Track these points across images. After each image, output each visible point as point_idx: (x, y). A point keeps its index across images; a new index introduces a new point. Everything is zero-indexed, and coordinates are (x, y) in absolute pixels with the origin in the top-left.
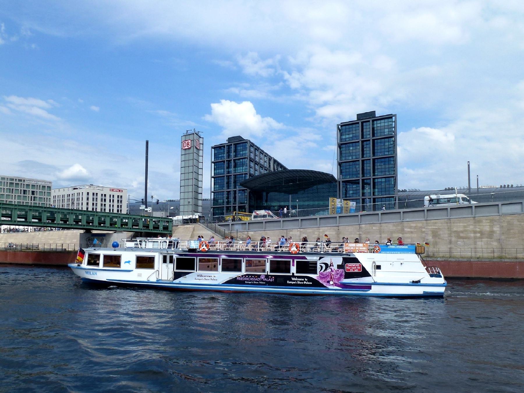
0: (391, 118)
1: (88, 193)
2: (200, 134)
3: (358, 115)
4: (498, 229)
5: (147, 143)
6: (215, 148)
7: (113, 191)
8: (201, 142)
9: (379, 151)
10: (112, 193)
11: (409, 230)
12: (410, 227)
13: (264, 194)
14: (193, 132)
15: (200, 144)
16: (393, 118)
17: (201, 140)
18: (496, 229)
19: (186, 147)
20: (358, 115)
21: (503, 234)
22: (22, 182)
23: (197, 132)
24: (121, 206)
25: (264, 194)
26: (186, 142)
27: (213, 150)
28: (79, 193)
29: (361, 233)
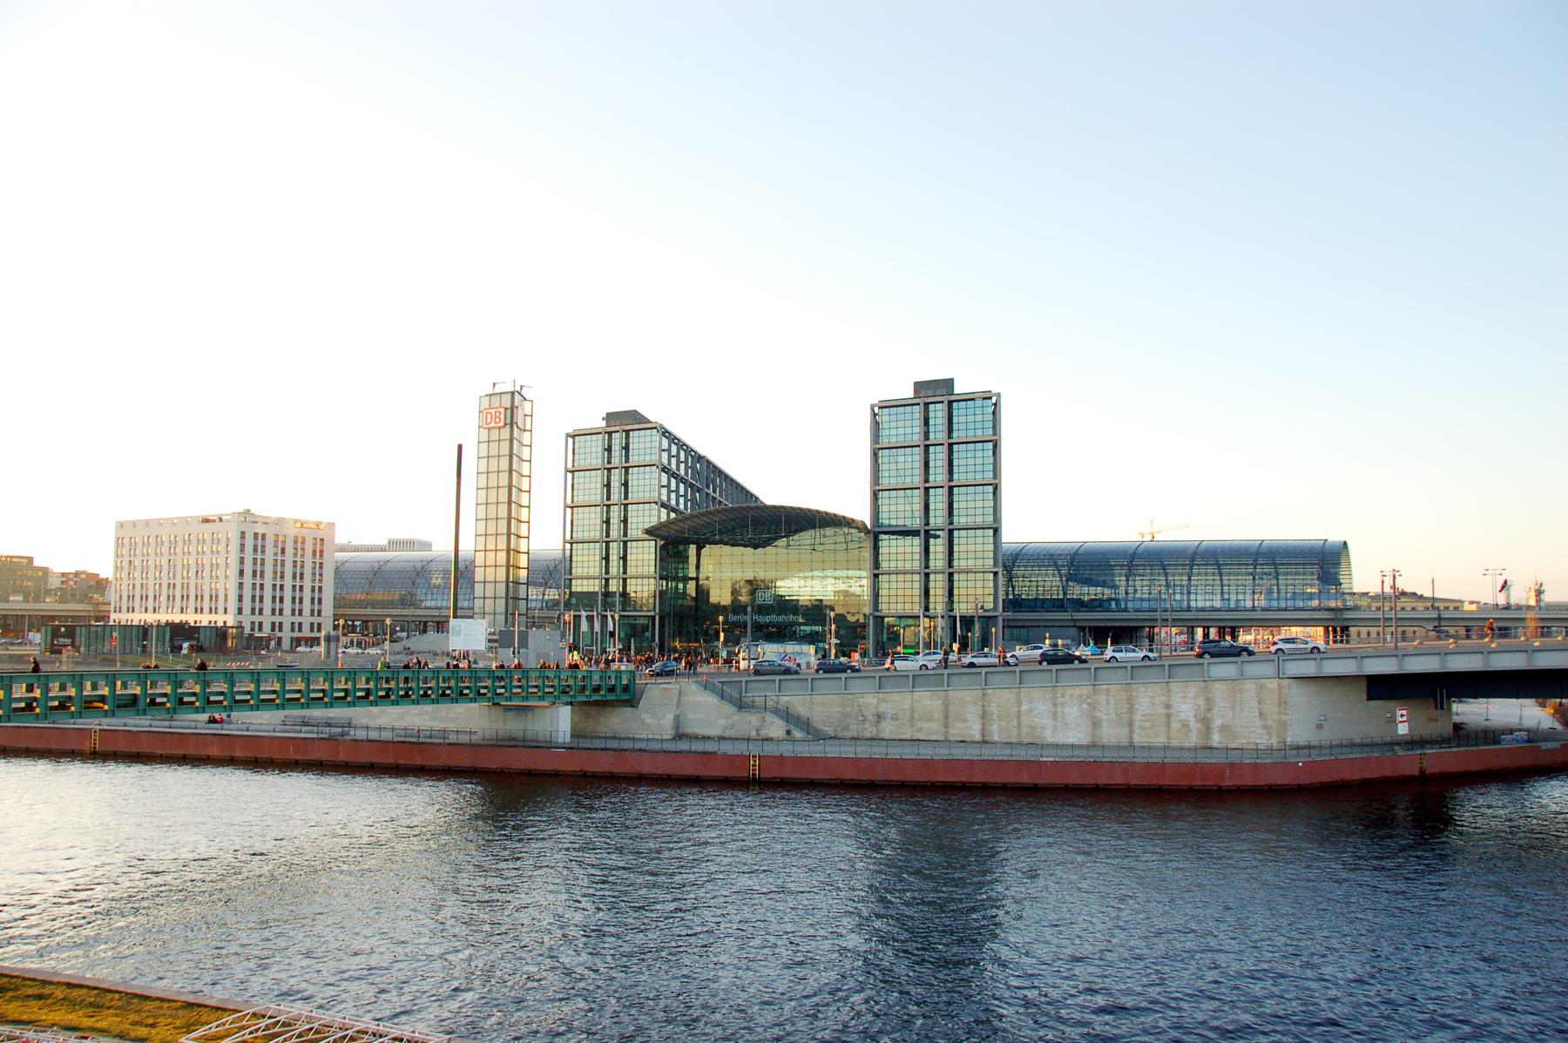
0: (990, 398)
3: (919, 386)
5: (460, 447)
13: (693, 549)
19: (493, 425)
23: (518, 389)
25: (693, 549)
26: (493, 411)
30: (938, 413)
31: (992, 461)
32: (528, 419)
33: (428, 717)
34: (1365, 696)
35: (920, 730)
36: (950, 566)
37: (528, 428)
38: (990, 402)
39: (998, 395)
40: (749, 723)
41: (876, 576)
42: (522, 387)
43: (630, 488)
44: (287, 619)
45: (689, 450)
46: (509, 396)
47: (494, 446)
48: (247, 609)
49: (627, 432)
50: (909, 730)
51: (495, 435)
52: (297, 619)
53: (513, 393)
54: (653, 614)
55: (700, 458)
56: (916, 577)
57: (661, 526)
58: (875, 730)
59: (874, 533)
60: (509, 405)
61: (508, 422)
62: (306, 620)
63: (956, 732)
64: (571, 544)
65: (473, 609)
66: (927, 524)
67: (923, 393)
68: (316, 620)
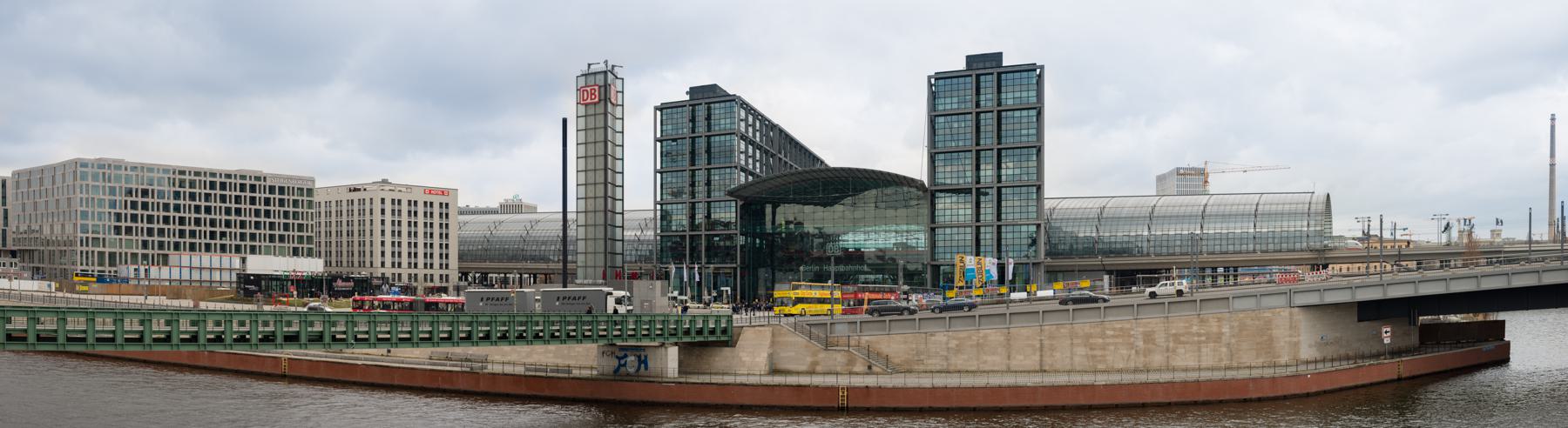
0: (1035, 70)
1: (383, 201)
3: (971, 60)
4: (1228, 330)
6: (662, 108)
7: (430, 193)
9: (1010, 133)
10: (429, 198)
11: (1112, 333)
12: (1114, 329)
13: (769, 209)
14: (602, 67)
16: (1038, 71)
17: (619, 82)
18: (1226, 330)
19: (589, 101)
20: (968, 57)
21: (1234, 336)
22: (262, 183)
24: (447, 225)
26: (589, 89)
27: (659, 113)
28: (364, 200)
29: (1043, 338)
30: (988, 83)
31: (1036, 126)
32: (620, 95)
33: (551, 355)
35: (985, 362)
36: (999, 219)
38: (1032, 74)
39: (1042, 67)
41: (933, 230)
42: (613, 66)
45: (763, 119)
46: (602, 76)
48: (388, 263)
50: (975, 363)
51: (591, 111)
52: (429, 271)
53: (605, 72)
54: (734, 265)
56: (968, 230)
57: (742, 188)
58: (945, 364)
59: (931, 191)
60: (602, 83)
61: (603, 97)
62: (436, 272)
63: (1019, 361)
64: (661, 205)
65: (576, 262)
66: (978, 182)
67: (975, 66)
68: (444, 272)
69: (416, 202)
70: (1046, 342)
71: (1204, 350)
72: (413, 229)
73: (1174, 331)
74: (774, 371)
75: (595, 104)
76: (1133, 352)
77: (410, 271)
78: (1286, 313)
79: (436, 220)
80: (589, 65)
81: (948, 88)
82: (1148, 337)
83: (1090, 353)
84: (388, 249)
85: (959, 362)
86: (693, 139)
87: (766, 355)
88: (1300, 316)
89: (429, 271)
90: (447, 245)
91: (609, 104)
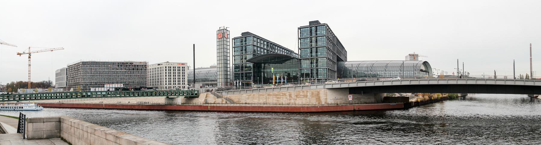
1: (166, 67)
2: (228, 29)
3: (310, 22)
8: (228, 34)
10: (179, 66)
12: (282, 93)
13: (263, 65)
15: (228, 35)
17: (228, 32)
19: (220, 37)
20: (309, 22)
23: (225, 28)
26: (219, 34)
27: (233, 40)
32: (229, 35)
34: (348, 93)
37: (229, 37)
40: (219, 100)
42: (227, 28)
43: (247, 51)
44: (172, 86)
45: (264, 40)
47: (220, 42)
49: (246, 37)
55: (268, 42)
60: (223, 33)
69: (175, 67)
70: (267, 97)
71: (303, 99)
72: (174, 74)
73: (296, 94)
74: (206, 103)
75: (221, 38)
76: (287, 99)
77: (169, 86)
78: (323, 90)
79: (181, 72)
80: (220, 28)
81: (321, 29)
82: (290, 96)
83: (277, 99)
84: (167, 80)
85: (248, 101)
86: (242, 47)
87: (204, 99)
88: (328, 91)
89: (175, 86)
90: (184, 78)
91: (225, 38)
